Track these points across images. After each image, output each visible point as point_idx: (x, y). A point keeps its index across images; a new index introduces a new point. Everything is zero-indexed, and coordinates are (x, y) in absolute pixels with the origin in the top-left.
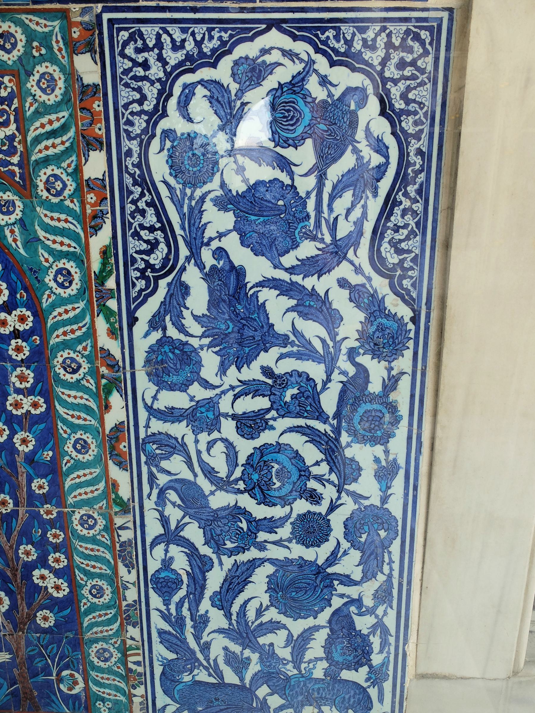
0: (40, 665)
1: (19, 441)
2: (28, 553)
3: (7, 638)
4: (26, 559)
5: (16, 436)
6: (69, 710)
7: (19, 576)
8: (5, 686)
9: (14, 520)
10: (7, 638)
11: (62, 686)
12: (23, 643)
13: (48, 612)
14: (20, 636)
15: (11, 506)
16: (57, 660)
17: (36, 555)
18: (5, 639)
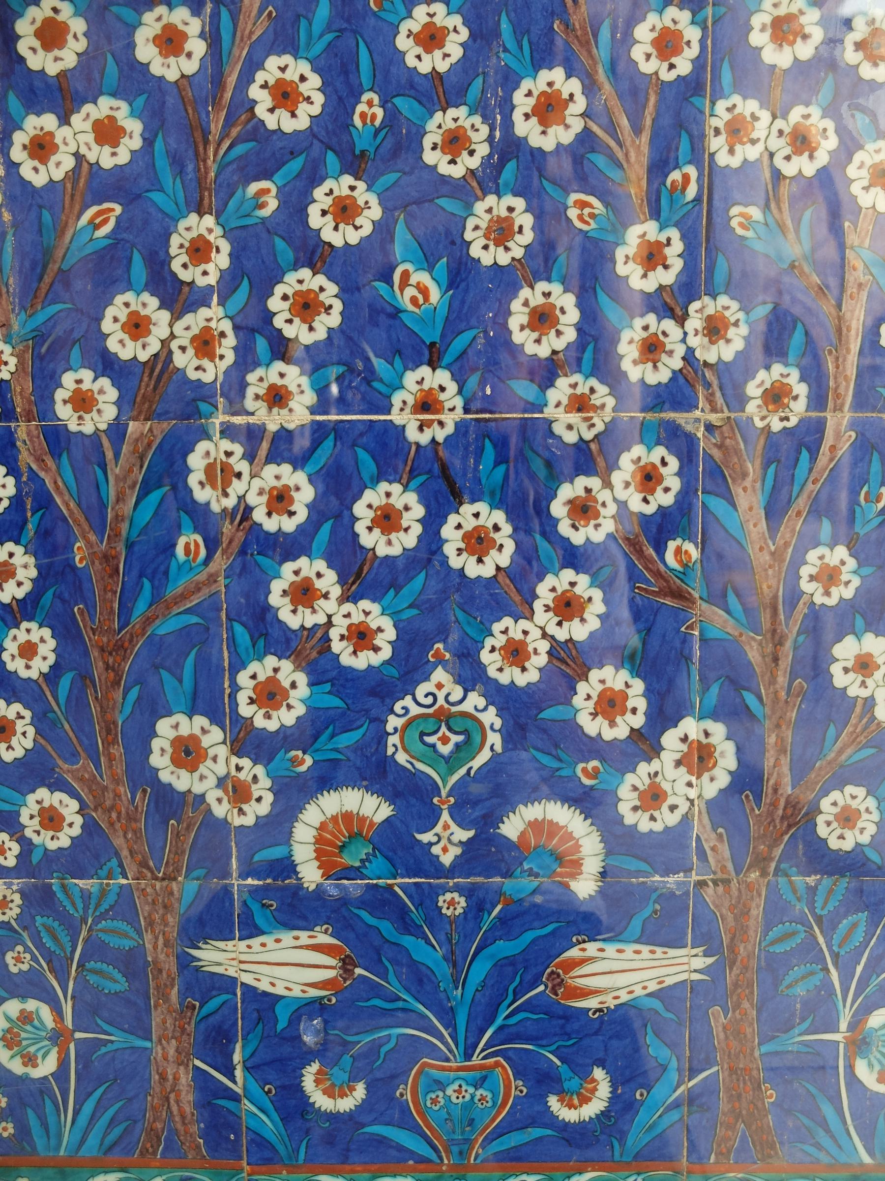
0: (800, 990)
1: (864, 173)
2: (829, 577)
3: (709, 893)
4: (819, 599)
5: (858, 157)
6: (870, 1152)
7: (786, 663)
8: (674, 1076)
9: (805, 455)
10: (709, 893)
11: (862, 1069)
12: (757, 911)
13: (861, 792)
14: (749, 887)
15: (799, 408)
16: (859, 969)
17: (856, 582)
18: (700, 901)
